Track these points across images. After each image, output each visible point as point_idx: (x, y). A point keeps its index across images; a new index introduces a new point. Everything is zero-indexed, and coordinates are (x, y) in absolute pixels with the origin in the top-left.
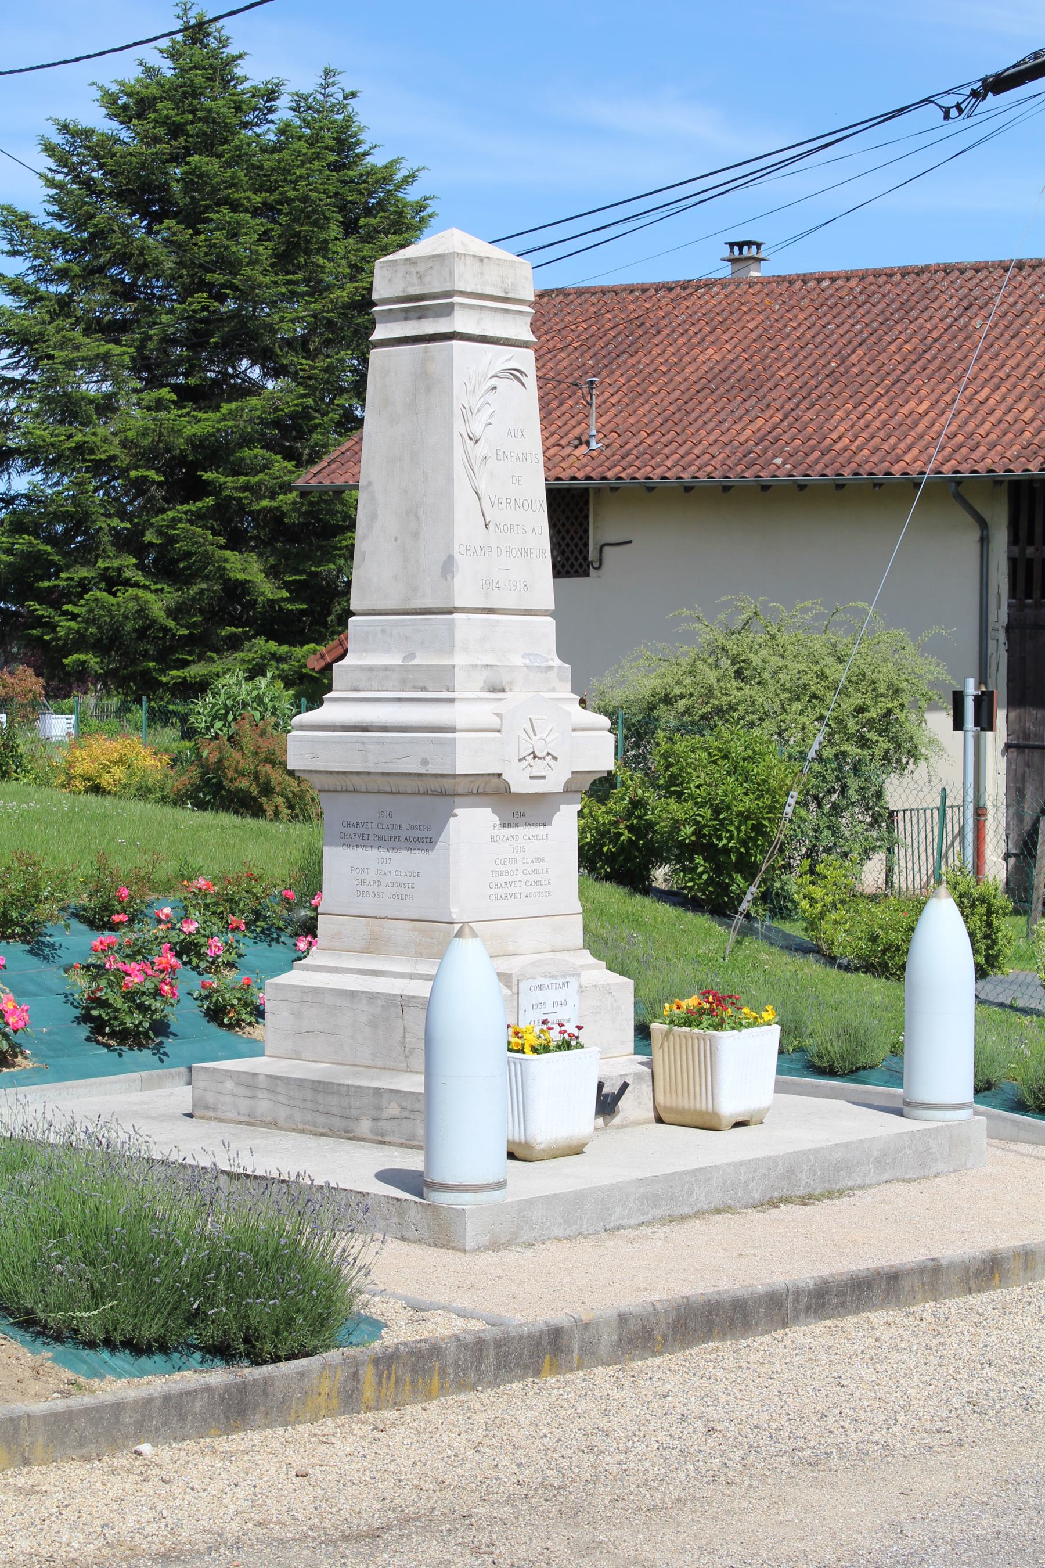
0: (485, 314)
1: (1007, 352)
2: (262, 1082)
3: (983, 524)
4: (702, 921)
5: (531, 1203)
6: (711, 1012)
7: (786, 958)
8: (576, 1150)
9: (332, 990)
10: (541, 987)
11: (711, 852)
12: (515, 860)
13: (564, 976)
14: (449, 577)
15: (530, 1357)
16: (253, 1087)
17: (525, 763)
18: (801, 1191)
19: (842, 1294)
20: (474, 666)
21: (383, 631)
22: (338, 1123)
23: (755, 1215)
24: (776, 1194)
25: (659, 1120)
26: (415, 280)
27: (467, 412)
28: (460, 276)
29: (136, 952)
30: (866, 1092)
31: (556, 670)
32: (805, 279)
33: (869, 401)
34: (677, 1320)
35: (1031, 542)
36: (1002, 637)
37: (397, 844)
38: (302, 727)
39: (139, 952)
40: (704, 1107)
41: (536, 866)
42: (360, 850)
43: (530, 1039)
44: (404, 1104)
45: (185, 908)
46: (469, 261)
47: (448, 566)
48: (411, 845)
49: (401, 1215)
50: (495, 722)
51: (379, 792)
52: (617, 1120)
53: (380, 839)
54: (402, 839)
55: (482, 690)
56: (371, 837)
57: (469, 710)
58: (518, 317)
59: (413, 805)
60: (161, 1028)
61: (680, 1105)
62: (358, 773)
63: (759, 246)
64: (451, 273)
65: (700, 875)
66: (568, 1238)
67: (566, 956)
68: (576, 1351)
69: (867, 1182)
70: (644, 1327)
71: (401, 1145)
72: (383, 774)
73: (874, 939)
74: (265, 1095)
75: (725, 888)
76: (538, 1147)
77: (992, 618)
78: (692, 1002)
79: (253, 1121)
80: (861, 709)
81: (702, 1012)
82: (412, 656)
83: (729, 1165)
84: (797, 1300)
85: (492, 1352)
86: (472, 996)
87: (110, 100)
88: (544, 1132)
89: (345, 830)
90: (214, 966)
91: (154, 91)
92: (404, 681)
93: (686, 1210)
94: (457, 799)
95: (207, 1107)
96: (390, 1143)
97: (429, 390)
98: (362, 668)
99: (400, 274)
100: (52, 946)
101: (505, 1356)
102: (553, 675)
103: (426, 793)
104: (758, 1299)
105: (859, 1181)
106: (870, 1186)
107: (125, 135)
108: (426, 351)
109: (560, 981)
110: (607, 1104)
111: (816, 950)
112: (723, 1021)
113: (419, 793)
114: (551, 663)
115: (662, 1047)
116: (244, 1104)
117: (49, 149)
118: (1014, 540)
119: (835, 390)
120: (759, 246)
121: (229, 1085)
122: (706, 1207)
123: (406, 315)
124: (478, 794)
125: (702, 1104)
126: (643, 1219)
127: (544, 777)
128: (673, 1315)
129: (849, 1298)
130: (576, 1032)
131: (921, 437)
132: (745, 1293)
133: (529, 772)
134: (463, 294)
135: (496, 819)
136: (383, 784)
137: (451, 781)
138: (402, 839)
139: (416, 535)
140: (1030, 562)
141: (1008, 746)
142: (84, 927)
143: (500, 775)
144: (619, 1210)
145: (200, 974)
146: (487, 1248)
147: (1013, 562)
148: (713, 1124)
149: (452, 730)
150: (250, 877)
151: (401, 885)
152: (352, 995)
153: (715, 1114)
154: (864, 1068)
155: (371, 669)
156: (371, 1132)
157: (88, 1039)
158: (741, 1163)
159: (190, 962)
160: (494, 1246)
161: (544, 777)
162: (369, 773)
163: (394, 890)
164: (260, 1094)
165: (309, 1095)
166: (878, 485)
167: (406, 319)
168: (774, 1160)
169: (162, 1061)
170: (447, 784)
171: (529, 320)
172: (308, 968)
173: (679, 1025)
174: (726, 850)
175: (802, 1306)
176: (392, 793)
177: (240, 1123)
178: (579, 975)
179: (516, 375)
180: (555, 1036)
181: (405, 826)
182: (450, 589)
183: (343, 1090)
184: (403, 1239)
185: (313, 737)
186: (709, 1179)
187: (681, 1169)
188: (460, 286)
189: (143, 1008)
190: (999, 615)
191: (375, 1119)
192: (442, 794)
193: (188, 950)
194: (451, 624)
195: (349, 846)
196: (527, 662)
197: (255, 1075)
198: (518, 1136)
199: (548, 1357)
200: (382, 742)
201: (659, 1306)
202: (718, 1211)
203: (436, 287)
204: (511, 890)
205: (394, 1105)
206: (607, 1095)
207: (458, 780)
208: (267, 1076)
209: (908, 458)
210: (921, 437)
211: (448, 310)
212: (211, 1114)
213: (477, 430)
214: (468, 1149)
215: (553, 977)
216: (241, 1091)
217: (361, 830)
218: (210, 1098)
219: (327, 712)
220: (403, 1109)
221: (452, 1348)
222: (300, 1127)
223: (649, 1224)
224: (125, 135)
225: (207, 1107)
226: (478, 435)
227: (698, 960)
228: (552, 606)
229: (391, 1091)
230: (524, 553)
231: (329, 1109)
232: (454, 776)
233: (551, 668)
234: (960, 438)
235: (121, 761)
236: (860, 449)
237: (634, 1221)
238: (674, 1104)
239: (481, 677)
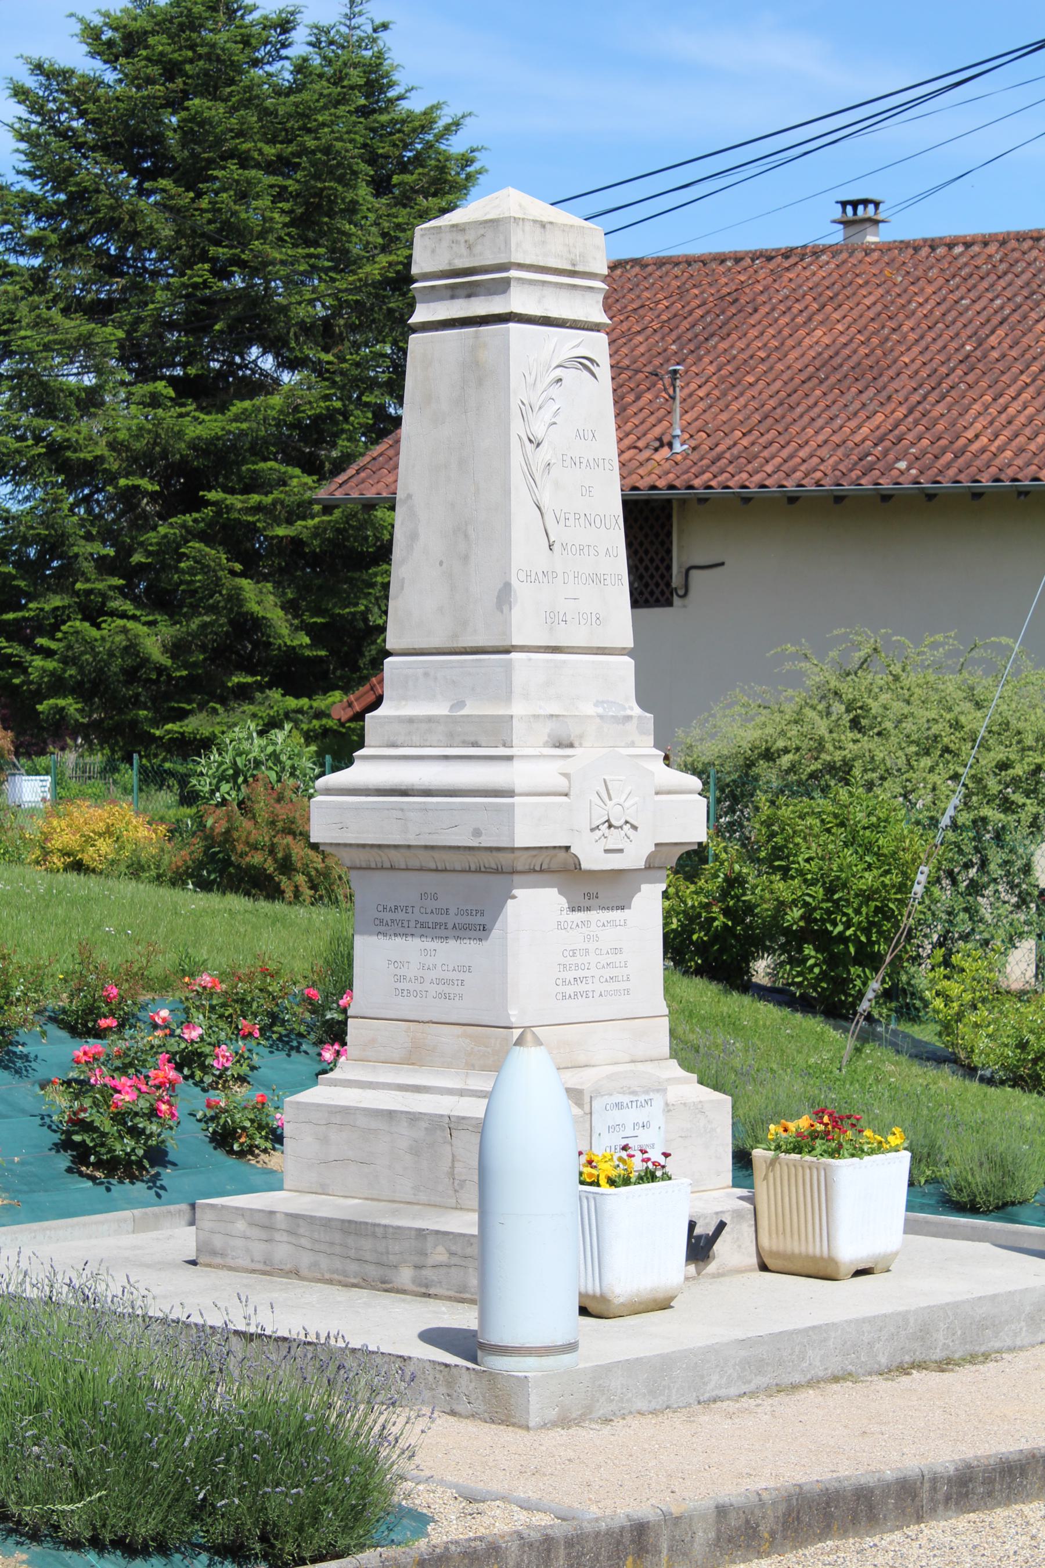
0: (548, 291)
2: (280, 1222)
4: (815, 1024)
5: (608, 1369)
6: (826, 1135)
7: (916, 1069)
8: (663, 1304)
9: (365, 1109)
10: (619, 1106)
11: (823, 941)
12: (587, 951)
13: (647, 1092)
14: (505, 608)
15: (609, 1558)
16: (268, 1228)
17: (598, 833)
18: (938, 1355)
19: (989, 1481)
20: (536, 717)
21: (426, 674)
22: (373, 1272)
23: (882, 1385)
24: (907, 1358)
25: (764, 1267)
26: (464, 251)
27: (527, 410)
28: (518, 245)
29: (127, 1065)
30: (1015, 1233)
31: (635, 721)
32: (933, 245)
33: (1012, 391)
34: (788, 1513)
37: (444, 933)
38: (328, 791)
39: (131, 1065)
40: (818, 1253)
41: (611, 958)
42: (398, 940)
43: (606, 1169)
44: (453, 1248)
45: (187, 1010)
46: (528, 227)
47: (504, 596)
49: (450, 1384)
50: (562, 783)
51: (421, 869)
52: (712, 1267)
54: (450, 926)
55: (546, 745)
56: (412, 924)
57: (530, 770)
58: (589, 295)
59: (463, 885)
60: (158, 1156)
61: (789, 1250)
62: (396, 847)
63: (877, 204)
64: (507, 242)
65: (811, 969)
66: (654, 1412)
67: (649, 1068)
68: (665, 1552)
69: (1018, 1343)
70: (747, 1522)
71: (450, 1298)
72: (426, 847)
73: (1023, 1046)
74: (285, 1237)
75: (842, 984)
76: (617, 1301)
78: (804, 1123)
79: (269, 1270)
80: (1004, 765)
81: (814, 1135)
82: (461, 704)
83: (849, 1322)
84: (934, 1489)
85: (562, 1552)
86: (535, 1117)
87: (92, 35)
88: (624, 1282)
89: (381, 915)
90: (221, 1080)
91: (144, 23)
92: (451, 735)
93: (797, 1378)
94: (516, 878)
95: (214, 1253)
96: (436, 1296)
97: (480, 382)
98: (400, 720)
99: (445, 244)
100: (25, 1057)
101: (578, 1557)
103: (478, 871)
104: (887, 1488)
105: (1009, 1342)
106: (1021, 1348)
107: (110, 77)
108: (477, 336)
109: (642, 1098)
110: (699, 1248)
111: (952, 1060)
112: (840, 1146)
113: (470, 871)
114: (629, 712)
115: (766, 1178)
116: (258, 1249)
117: (20, 93)
119: (970, 378)
120: (877, 204)
121: (241, 1226)
122: (821, 1374)
123: (453, 293)
124: (541, 871)
125: (816, 1248)
126: (745, 1388)
127: (621, 851)
128: (782, 1508)
129: (997, 1487)
130: (662, 1160)
132: (870, 1480)
134: (521, 266)
135: (563, 902)
136: (427, 860)
137: (509, 856)
138: (450, 926)
139: (466, 558)
142: (64, 1034)
143: (568, 848)
144: (715, 1378)
145: (204, 1090)
146: (554, 1424)
148: (829, 1271)
149: (510, 793)
150: (265, 972)
151: (450, 982)
152: (390, 1115)
153: (831, 1260)
154: (1013, 1204)
155: (411, 720)
156: (414, 1282)
157: (69, 1170)
158: (864, 1320)
159: (192, 1076)
160: (564, 1422)
161: (621, 851)
162: (409, 847)
163: (440, 988)
164: (278, 1236)
165: (337, 1237)
167: (453, 297)
168: (904, 1316)
169: (159, 1196)
170: (504, 859)
171: (600, 297)
172: (335, 1083)
173: (787, 1152)
174: (842, 938)
175: (940, 1496)
176: (437, 870)
177: (253, 1271)
178: (665, 1090)
179: (586, 364)
180: (637, 1165)
182: (507, 623)
183: (379, 1231)
184: (453, 1413)
185: (342, 803)
186: (825, 1340)
187: (790, 1327)
188: (517, 257)
189: (136, 1132)
191: (418, 1267)
192: (498, 871)
193: (189, 1061)
194: (508, 667)
195: (385, 935)
196: (600, 710)
197: (272, 1213)
198: (592, 1287)
199: (630, 1559)
200: (425, 809)
201: (765, 1496)
202: (836, 1379)
203: (489, 260)
204: (582, 987)
205: (440, 1249)
206: (699, 1237)
207: (517, 854)
208: (287, 1214)
211: (503, 287)
212: (218, 1260)
213: (539, 430)
214: (533, 1306)
215: (634, 1093)
216: (255, 1232)
217: (400, 915)
218: (218, 1242)
219: (360, 772)
220: (452, 1254)
221: (514, 1547)
222: (327, 1276)
223: (752, 1394)
224: (110, 77)
225: (214, 1253)
226: (540, 436)
227: (809, 1072)
228: (630, 644)
229: (437, 1232)
230: (596, 579)
231: (364, 1257)
232: (513, 850)
233: (629, 718)
235: (108, 832)
236: (1002, 449)
237: (733, 1391)
238: (781, 1248)
239: (544, 731)
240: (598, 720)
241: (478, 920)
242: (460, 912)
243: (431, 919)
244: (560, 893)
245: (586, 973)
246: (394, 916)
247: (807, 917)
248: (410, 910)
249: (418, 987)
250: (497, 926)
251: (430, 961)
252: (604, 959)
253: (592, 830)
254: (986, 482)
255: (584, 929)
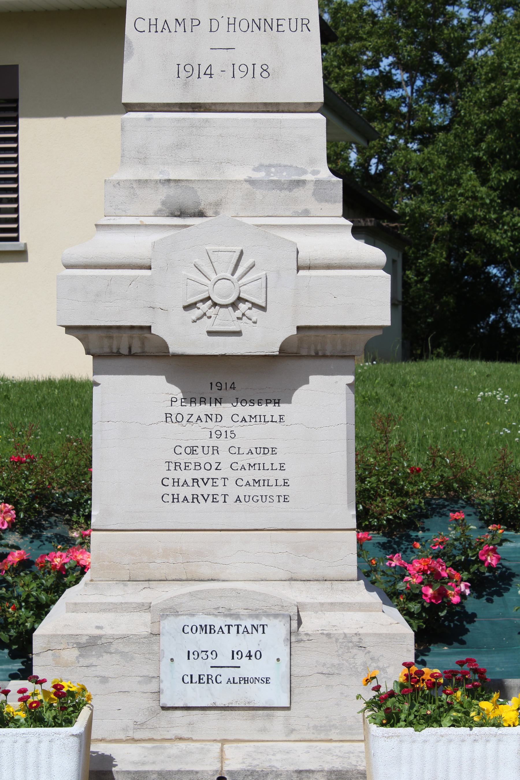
12: (216, 450)
13: (257, 616)
17: (195, 313)
20: (143, 183)
31: (310, 188)
55: (157, 214)
102: (304, 194)
124: (131, 355)
127: (238, 333)
133: (207, 325)
135: (176, 392)
143: (150, 327)
161: (238, 333)
204: (208, 490)
215: (237, 616)
228: (319, 97)
240: (247, 186)
244: (169, 381)
245: (213, 473)
252: (245, 460)
253: (188, 308)
255: (211, 424)
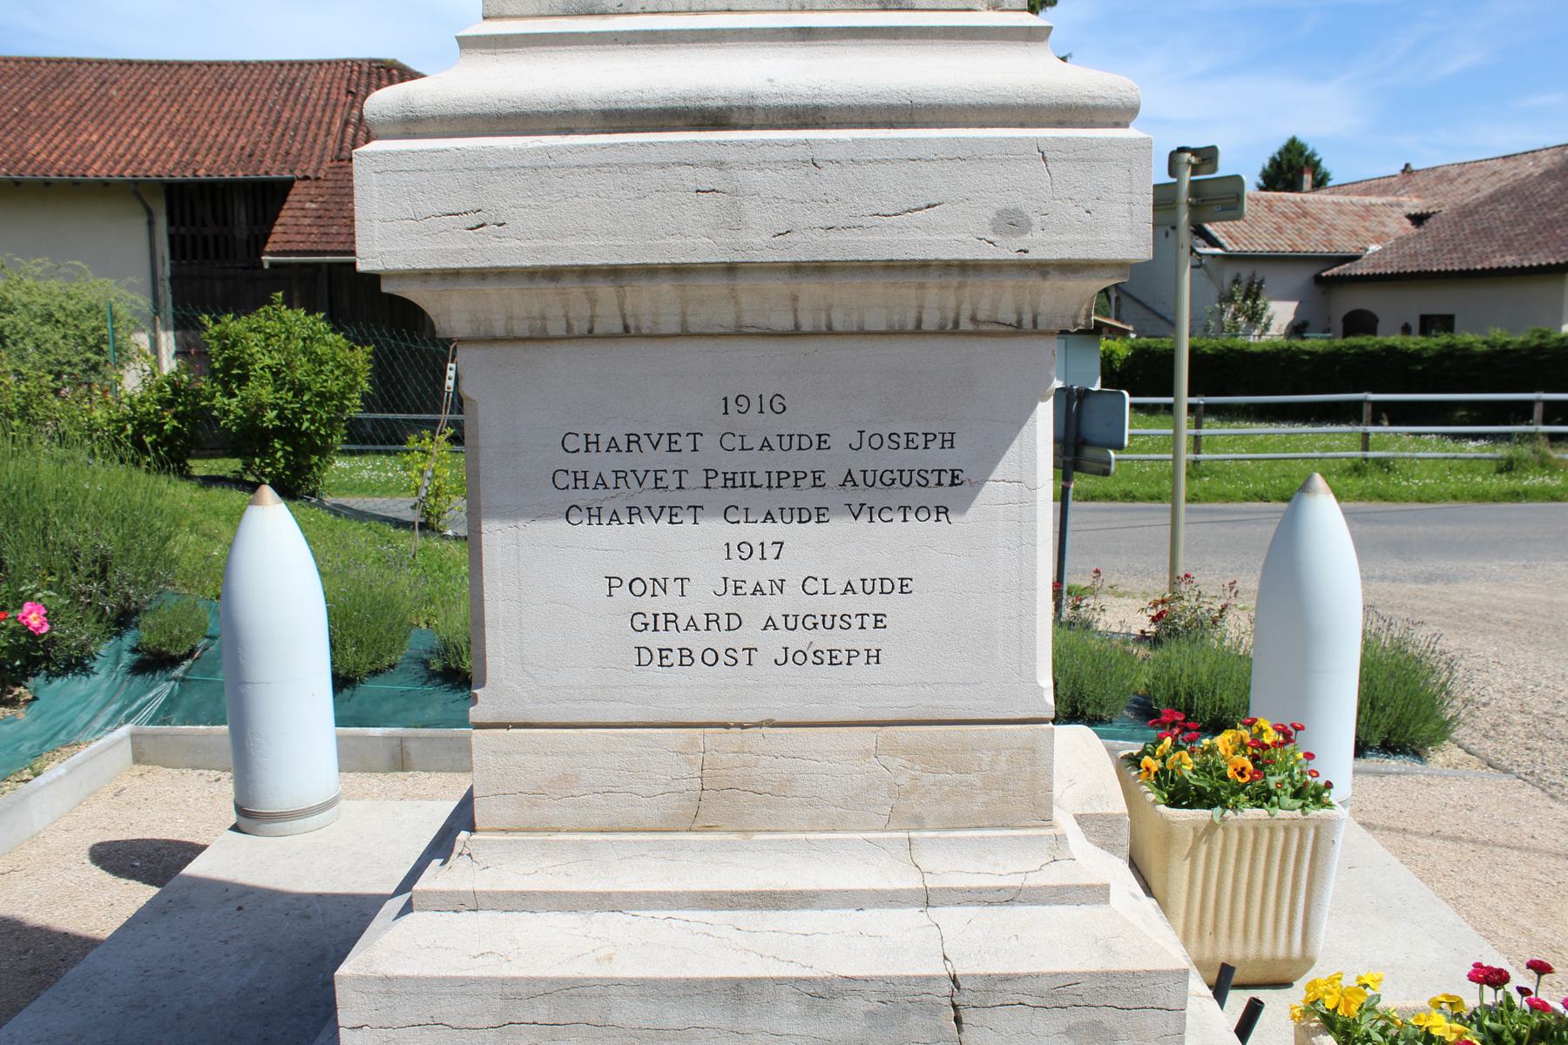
1: (140, 110)
3: (150, 213)
33: (52, 132)
35: (183, 224)
36: (167, 284)
48: (875, 497)
53: (730, 481)
54: (833, 477)
56: (694, 479)
77: (160, 272)
80: (95, 329)
89: (578, 462)
113: (918, 331)
118: (171, 222)
131: (100, 155)
136: (766, 304)
138: (833, 477)
140: (183, 237)
141: (177, 354)
147: (172, 238)
166: (76, 183)
181: (841, 438)
185: (480, 154)
190: (165, 270)
195: (594, 514)
209: (96, 166)
210: (100, 155)
234: (129, 157)
236: (57, 160)
241: (935, 457)
242: (865, 440)
243: (761, 463)
246: (624, 461)
247: (279, 417)
248: (685, 443)
249: (719, 639)
250: (1000, 471)
251: (756, 571)
254: (53, 176)
